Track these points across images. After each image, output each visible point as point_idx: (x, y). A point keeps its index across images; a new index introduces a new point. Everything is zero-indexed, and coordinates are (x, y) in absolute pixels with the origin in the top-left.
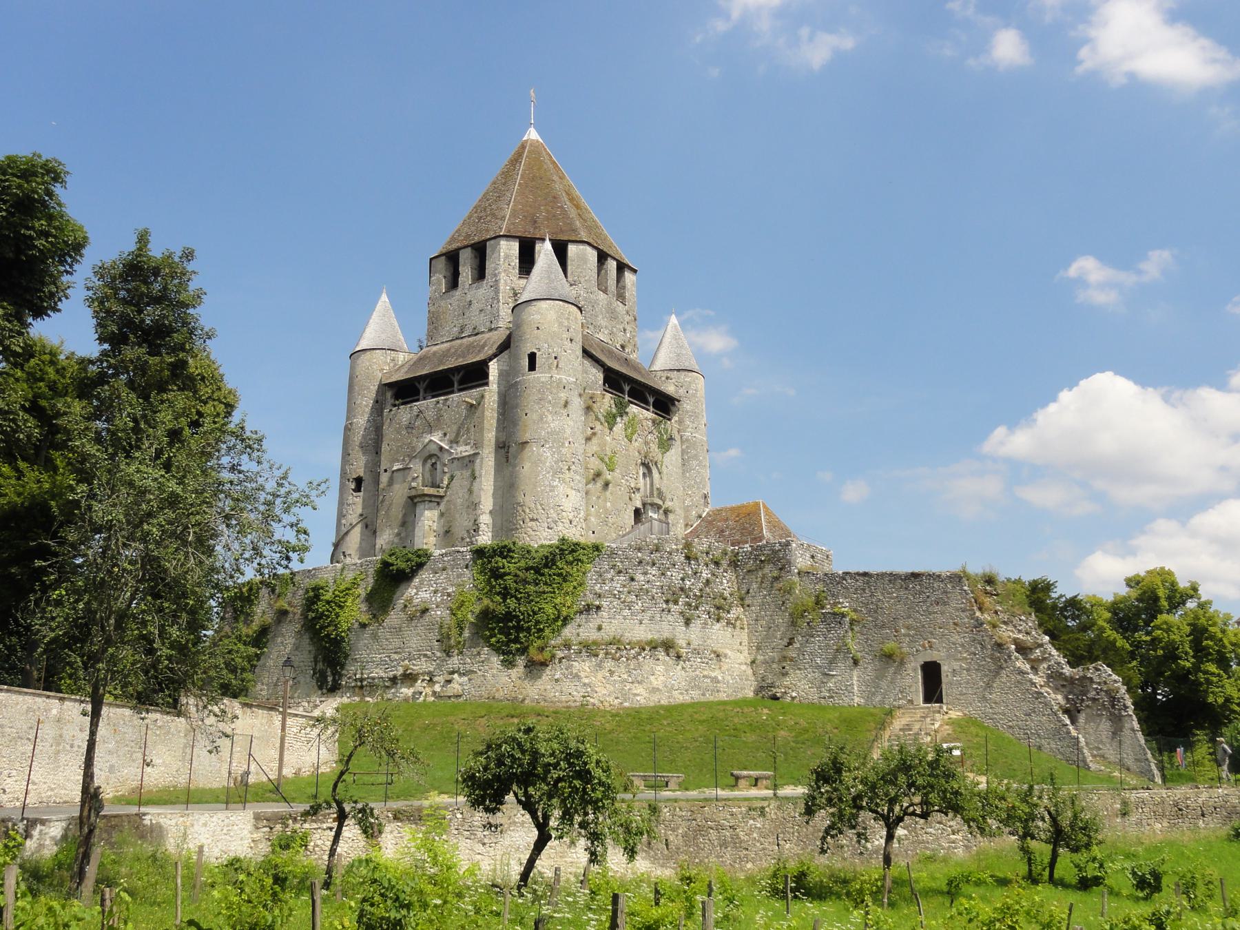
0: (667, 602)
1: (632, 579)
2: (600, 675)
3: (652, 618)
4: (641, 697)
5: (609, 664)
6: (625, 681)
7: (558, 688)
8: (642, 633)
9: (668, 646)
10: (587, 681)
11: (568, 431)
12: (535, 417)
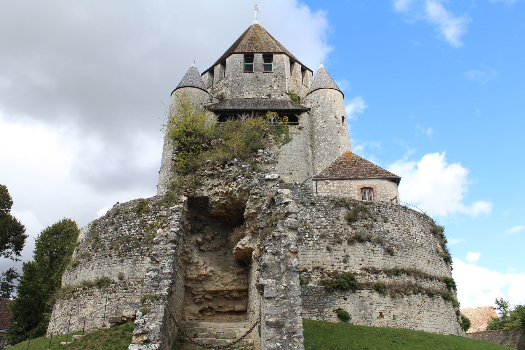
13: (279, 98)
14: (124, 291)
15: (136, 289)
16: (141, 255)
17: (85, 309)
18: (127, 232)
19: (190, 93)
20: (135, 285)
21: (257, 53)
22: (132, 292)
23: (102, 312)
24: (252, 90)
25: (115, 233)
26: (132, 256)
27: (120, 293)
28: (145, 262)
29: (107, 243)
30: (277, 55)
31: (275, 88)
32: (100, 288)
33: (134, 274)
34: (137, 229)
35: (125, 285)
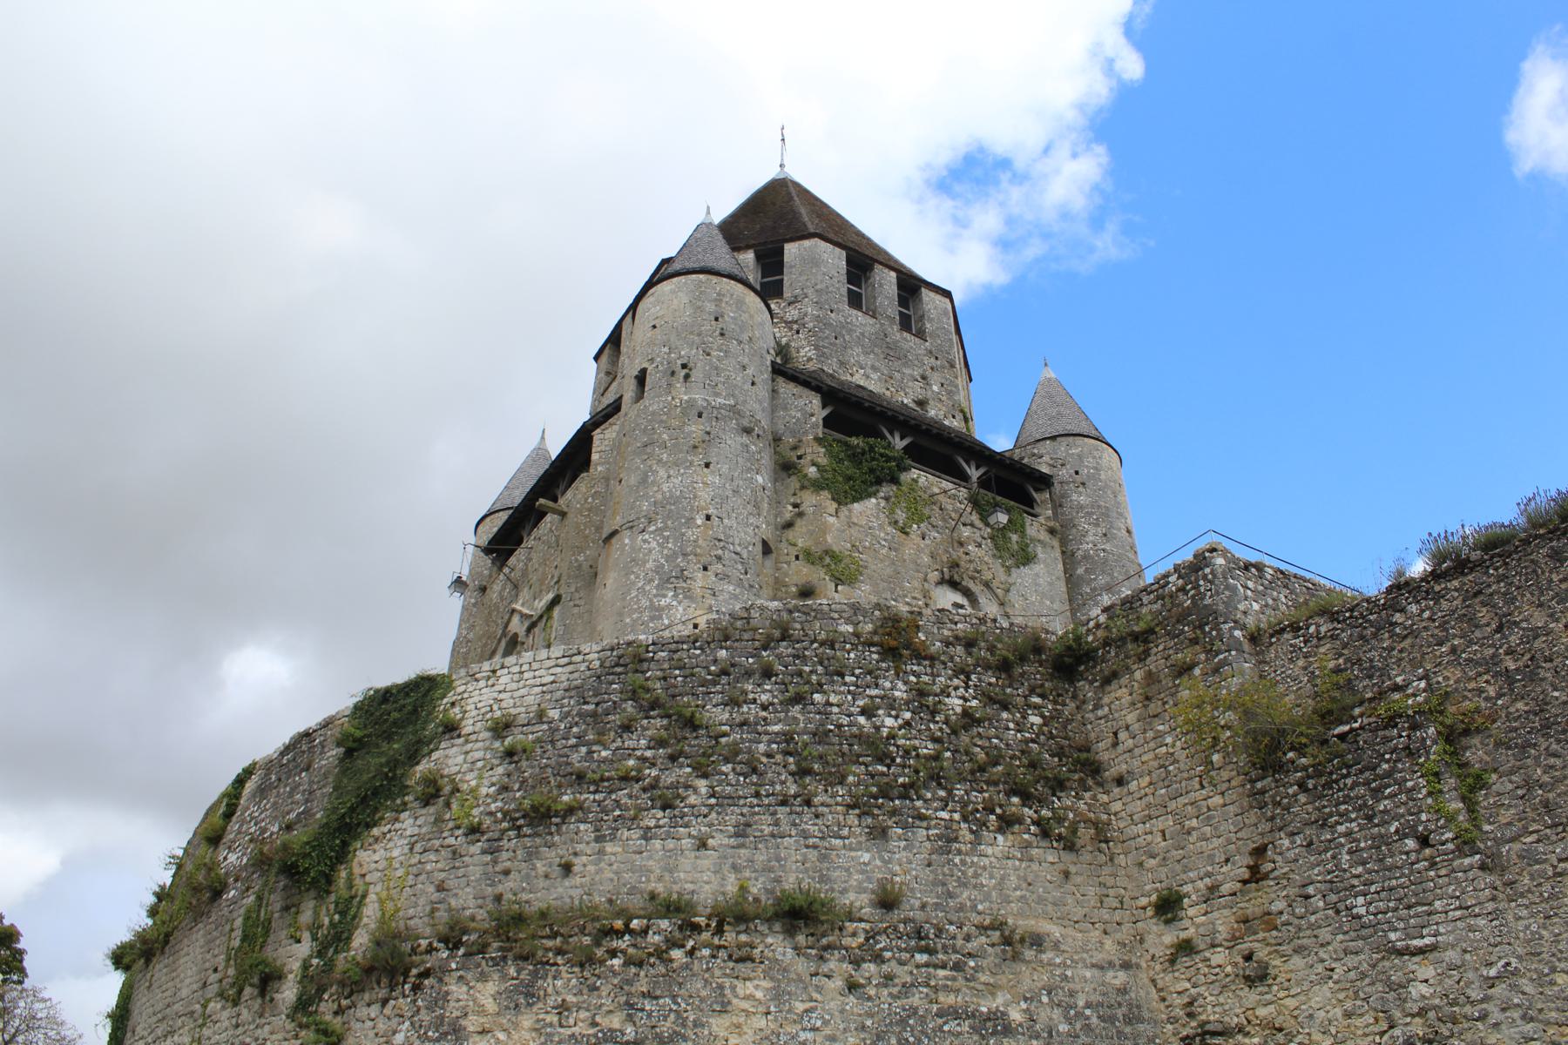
0: (802, 772)
1: (691, 724)
2: (527, 1021)
3: (741, 831)
5: (562, 983)
8: (705, 878)
9: (799, 916)
11: (705, 495)
12: (633, 480)
13: (946, 423)
14: (921, 958)
15: (970, 955)
16: (965, 819)
18: (862, 720)
19: (740, 303)
20: (968, 938)
22: (957, 967)
24: (874, 368)
25: (796, 711)
26: (922, 817)
27: (902, 963)
28: (990, 851)
29: (762, 747)
30: (932, 294)
31: (935, 388)
32: (790, 932)
33: (950, 895)
34: (908, 715)
35: (919, 934)
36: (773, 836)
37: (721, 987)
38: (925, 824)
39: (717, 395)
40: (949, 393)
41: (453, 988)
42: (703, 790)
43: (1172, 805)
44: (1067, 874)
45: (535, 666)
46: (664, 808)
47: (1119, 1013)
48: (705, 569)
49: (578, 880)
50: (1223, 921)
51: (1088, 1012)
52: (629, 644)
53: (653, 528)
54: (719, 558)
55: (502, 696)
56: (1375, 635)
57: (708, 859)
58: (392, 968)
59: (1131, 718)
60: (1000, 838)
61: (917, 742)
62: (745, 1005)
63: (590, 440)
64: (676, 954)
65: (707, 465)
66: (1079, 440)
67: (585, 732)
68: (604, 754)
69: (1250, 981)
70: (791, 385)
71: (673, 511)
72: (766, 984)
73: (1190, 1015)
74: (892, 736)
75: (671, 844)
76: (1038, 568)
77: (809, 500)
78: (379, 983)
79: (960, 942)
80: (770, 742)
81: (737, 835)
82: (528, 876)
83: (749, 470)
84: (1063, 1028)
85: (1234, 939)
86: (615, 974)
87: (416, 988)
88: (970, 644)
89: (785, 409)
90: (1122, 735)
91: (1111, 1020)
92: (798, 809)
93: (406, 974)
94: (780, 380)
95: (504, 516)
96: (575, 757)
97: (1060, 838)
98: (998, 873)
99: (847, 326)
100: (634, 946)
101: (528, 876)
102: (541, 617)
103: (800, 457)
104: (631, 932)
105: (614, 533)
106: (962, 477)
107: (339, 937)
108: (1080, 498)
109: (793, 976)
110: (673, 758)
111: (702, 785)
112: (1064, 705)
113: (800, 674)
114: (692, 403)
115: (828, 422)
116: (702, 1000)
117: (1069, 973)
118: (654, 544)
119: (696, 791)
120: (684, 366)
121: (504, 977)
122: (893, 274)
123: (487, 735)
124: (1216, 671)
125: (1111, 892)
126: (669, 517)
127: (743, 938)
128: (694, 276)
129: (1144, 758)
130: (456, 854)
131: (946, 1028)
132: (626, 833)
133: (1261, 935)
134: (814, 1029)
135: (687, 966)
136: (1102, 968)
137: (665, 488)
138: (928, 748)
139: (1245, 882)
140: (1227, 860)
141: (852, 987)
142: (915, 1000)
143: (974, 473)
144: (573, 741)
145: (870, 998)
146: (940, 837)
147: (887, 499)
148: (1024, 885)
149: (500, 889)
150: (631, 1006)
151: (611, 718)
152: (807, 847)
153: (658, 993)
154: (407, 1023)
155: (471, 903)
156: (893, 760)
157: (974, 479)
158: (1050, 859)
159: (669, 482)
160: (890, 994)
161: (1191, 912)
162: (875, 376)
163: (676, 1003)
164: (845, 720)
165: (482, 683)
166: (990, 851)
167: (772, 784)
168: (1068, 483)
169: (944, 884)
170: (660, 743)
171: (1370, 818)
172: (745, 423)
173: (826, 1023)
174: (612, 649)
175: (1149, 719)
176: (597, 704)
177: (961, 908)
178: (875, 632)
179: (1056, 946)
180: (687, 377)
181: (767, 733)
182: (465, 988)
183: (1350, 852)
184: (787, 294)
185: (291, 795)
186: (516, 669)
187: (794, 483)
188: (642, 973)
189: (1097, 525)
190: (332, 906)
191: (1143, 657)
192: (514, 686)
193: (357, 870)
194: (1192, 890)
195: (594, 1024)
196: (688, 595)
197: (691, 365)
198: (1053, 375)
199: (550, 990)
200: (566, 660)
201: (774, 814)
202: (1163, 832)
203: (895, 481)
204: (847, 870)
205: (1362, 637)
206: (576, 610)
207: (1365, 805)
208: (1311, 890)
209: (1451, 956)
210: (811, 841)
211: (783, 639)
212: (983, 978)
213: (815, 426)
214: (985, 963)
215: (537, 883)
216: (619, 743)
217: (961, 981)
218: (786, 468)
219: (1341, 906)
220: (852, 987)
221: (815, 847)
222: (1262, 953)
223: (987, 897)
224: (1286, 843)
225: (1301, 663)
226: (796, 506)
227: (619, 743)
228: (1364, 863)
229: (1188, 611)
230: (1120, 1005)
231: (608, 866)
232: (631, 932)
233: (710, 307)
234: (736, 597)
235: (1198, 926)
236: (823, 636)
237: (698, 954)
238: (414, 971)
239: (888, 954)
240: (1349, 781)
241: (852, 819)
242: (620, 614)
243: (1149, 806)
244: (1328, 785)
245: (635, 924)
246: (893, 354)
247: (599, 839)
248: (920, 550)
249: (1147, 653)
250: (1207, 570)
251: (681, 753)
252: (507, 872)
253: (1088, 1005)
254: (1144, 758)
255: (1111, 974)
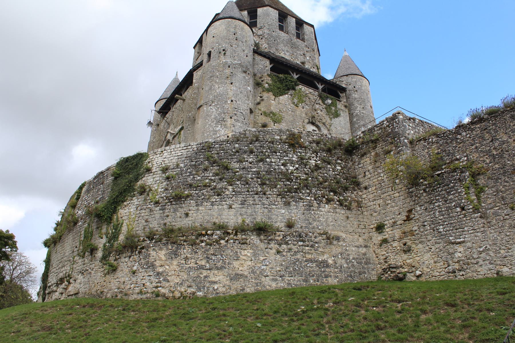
0: (263, 184)
1: (227, 168)
2: (175, 262)
4: (220, 283)
5: (186, 251)
6: (202, 267)
7: (134, 279)
8: (231, 217)
9: (261, 230)
10: (161, 270)
11: (231, 93)
12: (207, 89)
13: (311, 70)
14: (301, 243)
16: (315, 199)
17: (238, 262)
18: (282, 167)
19: (242, 29)
20: (315, 237)
21: (290, 15)
22: (312, 246)
23: (272, 268)
24: (287, 51)
26: (301, 199)
27: (294, 245)
28: (323, 210)
29: (250, 176)
30: (307, 26)
31: (308, 58)
32: (259, 235)
33: (310, 224)
34: (297, 166)
35: (300, 236)
36: (253, 204)
37: (237, 252)
38: (302, 201)
39: (235, 60)
40: (312, 60)
41: (152, 252)
42: (231, 190)
43: (382, 196)
44: (348, 218)
45: (175, 150)
46: (218, 196)
47: (363, 261)
48: (231, 118)
49: (190, 219)
50: (397, 233)
51: (353, 261)
52: (206, 142)
53: (214, 104)
54: (236, 114)
55: (165, 160)
56: (451, 142)
57: (232, 212)
58: (132, 246)
59: (370, 168)
60: (327, 206)
61: (300, 175)
62: (244, 258)
63: (193, 74)
64: (222, 242)
65: (232, 84)
66: (356, 76)
67: (192, 171)
68: (198, 178)
69: (405, 252)
70: (260, 57)
71: (220, 99)
72: (251, 251)
73: (386, 262)
74: (292, 173)
75: (220, 207)
76: (341, 118)
77: (265, 95)
78: (128, 251)
79: (313, 239)
80: (252, 174)
81: (241, 204)
82: (174, 217)
83: (245, 85)
84: (345, 265)
85: (401, 239)
86: (203, 248)
87: (140, 252)
88: (318, 143)
89: (257, 65)
90: (367, 173)
91: (360, 263)
92: (261, 196)
93: (136, 248)
94: (256, 55)
95: (164, 101)
96: (189, 179)
97: (346, 206)
98: (326, 217)
99: (278, 37)
100: (209, 239)
101: (174, 217)
102: (177, 134)
103: (262, 81)
104: (208, 235)
105: (201, 106)
106: (316, 88)
107: (115, 237)
108: (355, 95)
109: (259, 249)
110: (221, 180)
111: (230, 188)
112: (348, 163)
113: (262, 152)
114: (226, 63)
115: (272, 69)
116: (230, 256)
117: (348, 249)
118: (214, 110)
119: (228, 190)
120: (224, 50)
121: (168, 249)
122: (294, 19)
123: (160, 172)
124: (398, 153)
125: (362, 223)
126: (219, 101)
127: (244, 237)
128: (227, 19)
129: (374, 181)
130: (151, 210)
131: (308, 265)
132: (206, 204)
133: (409, 237)
134: (266, 265)
135: (226, 246)
136: (358, 247)
137: (218, 91)
138: (304, 177)
139: (405, 221)
140: (399, 214)
141: (278, 252)
142: (299, 256)
143: (320, 87)
144: (188, 174)
145: (284, 256)
146: (307, 205)
147: (291, 95)
148: (334, 221)
149: (165, 221)
150: (208, 258)
151: (201, 166)
152: (264, 208)
153: (217, 254)
154: (137, 263)
155: (157, 226)
156: (292, 180)
157: (320, 89)
158: (343, 212)
159: (219, 89)
160: (291, 255)
161: (387, 230)
162: (288, 54)
163: (222, 257)
164: (277, 167)
165: (158, 155)
166: (323, 210)
167: (253, 188)
168: (351, 90)
169: (308, 220)
170: (217, 174)
171: (446, 201)
172: (244, 69)
173: (270, 263)
174: (201, 144)
175: (376, 168)
176: (196, 162)
177: (314, 228)
178: (287, 139)
179: (344, 240)
180: (225, 54)
181: (251, 171)
182: (155, 252)
183: (439, 212)
184: (258, 26)
185: (97, 192)
186: (169, 151)
187: (260, 89)
188: (211, 248)
189: (361, 105)
190: (112, 227)
191: (374, 148)
192: (169, 156)
193: (119, 216)
194: (388, 223)
195: (196, 263)
196: (225, 126)
197: (226, 50)
198: (347, 54)
199: (182, 253)
200: (186, 148)
201: (254, 197)
202: (379, 204)
203: (294, 89)
204: (277, 215)
205: (446, 143)
206: (189, 132)
207: (445, 197)
208: (426, 224)
209: (469, 244)
210: (266, 206)
211: (257, 141)
212: (320, 250)
213: (267, 70)
214: (321, 245)
215: (177, 219)
216: (203, 174)
217: (313, 251)
218: (258, 84)
219: (435, 229)
220: (278, 252)
221: (267, 208)
222: (409, 243)
223: (322, 225)
224: (419, 208)
225: (426, 151)
226: (261, 97)
227: (203, 174)
228: (443, 215)
229: (390, 134)
230: (363, 258)
231: (200, 214)
232: (208, 235)
233: (232, 30)
234: (241, 127)
235: (389, 234)
236: (270, 140)
237: (229, 242)
238: (139, 247)
239: (290, 242)
240: (440, 189)
241: (279, 199)
242: (203, 133)
243: (375, 196)
244: (433, 190)
245: (209, 232)
246: (294, 46)
247: (196, 206)
248: (302, 112)
249: (376, 147)
250: (397, 120)
251: (223, 178)
252: (168, 216)
253: (353, 259)
254: (374, 181)
255: (361, 249)
